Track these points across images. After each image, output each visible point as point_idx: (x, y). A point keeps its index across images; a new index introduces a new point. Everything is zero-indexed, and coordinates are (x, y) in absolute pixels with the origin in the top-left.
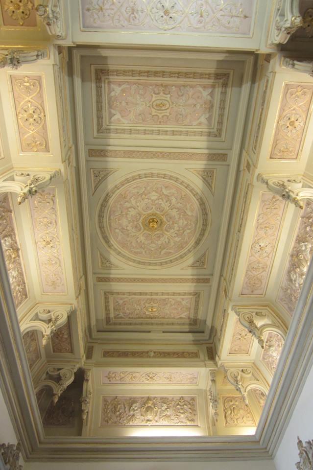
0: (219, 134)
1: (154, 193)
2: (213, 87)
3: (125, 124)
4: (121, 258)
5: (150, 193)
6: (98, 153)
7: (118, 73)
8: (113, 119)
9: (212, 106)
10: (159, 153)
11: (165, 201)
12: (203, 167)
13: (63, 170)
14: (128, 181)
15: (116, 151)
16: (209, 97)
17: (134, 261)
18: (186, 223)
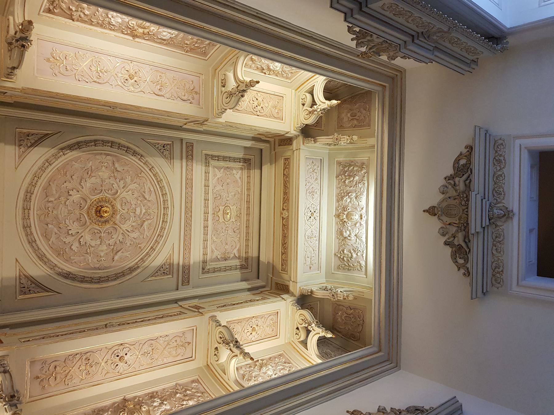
0: (204, 271)
1: (144, 211)
2: (239, 258)
3: (212, 182)
4: (40, 163)
5: (144, 206)
6: (189, 151)
7: (249, 177)
8: (216, 169)
9: (226, 260)
10: (190, 214)
11: (134, 224)
12: (176, 262)
13: (220, 120)
14: (159, 181)
15: (192, 170)
16: (232, 255)
17: (33, 184)
18: (102, 255)
